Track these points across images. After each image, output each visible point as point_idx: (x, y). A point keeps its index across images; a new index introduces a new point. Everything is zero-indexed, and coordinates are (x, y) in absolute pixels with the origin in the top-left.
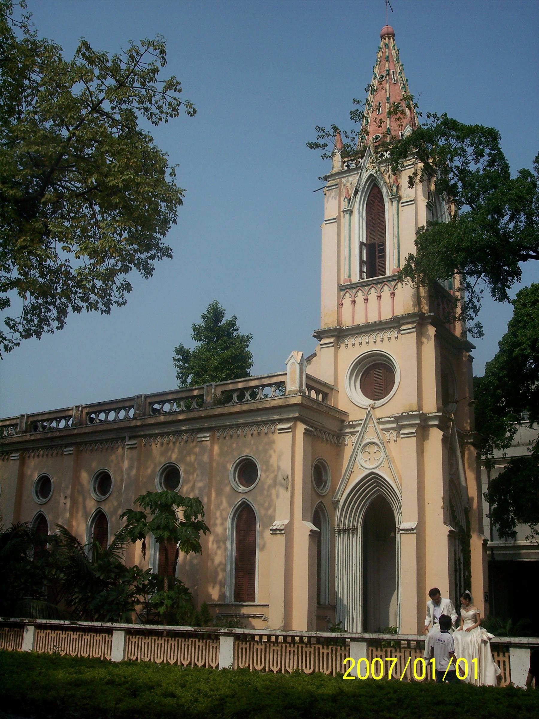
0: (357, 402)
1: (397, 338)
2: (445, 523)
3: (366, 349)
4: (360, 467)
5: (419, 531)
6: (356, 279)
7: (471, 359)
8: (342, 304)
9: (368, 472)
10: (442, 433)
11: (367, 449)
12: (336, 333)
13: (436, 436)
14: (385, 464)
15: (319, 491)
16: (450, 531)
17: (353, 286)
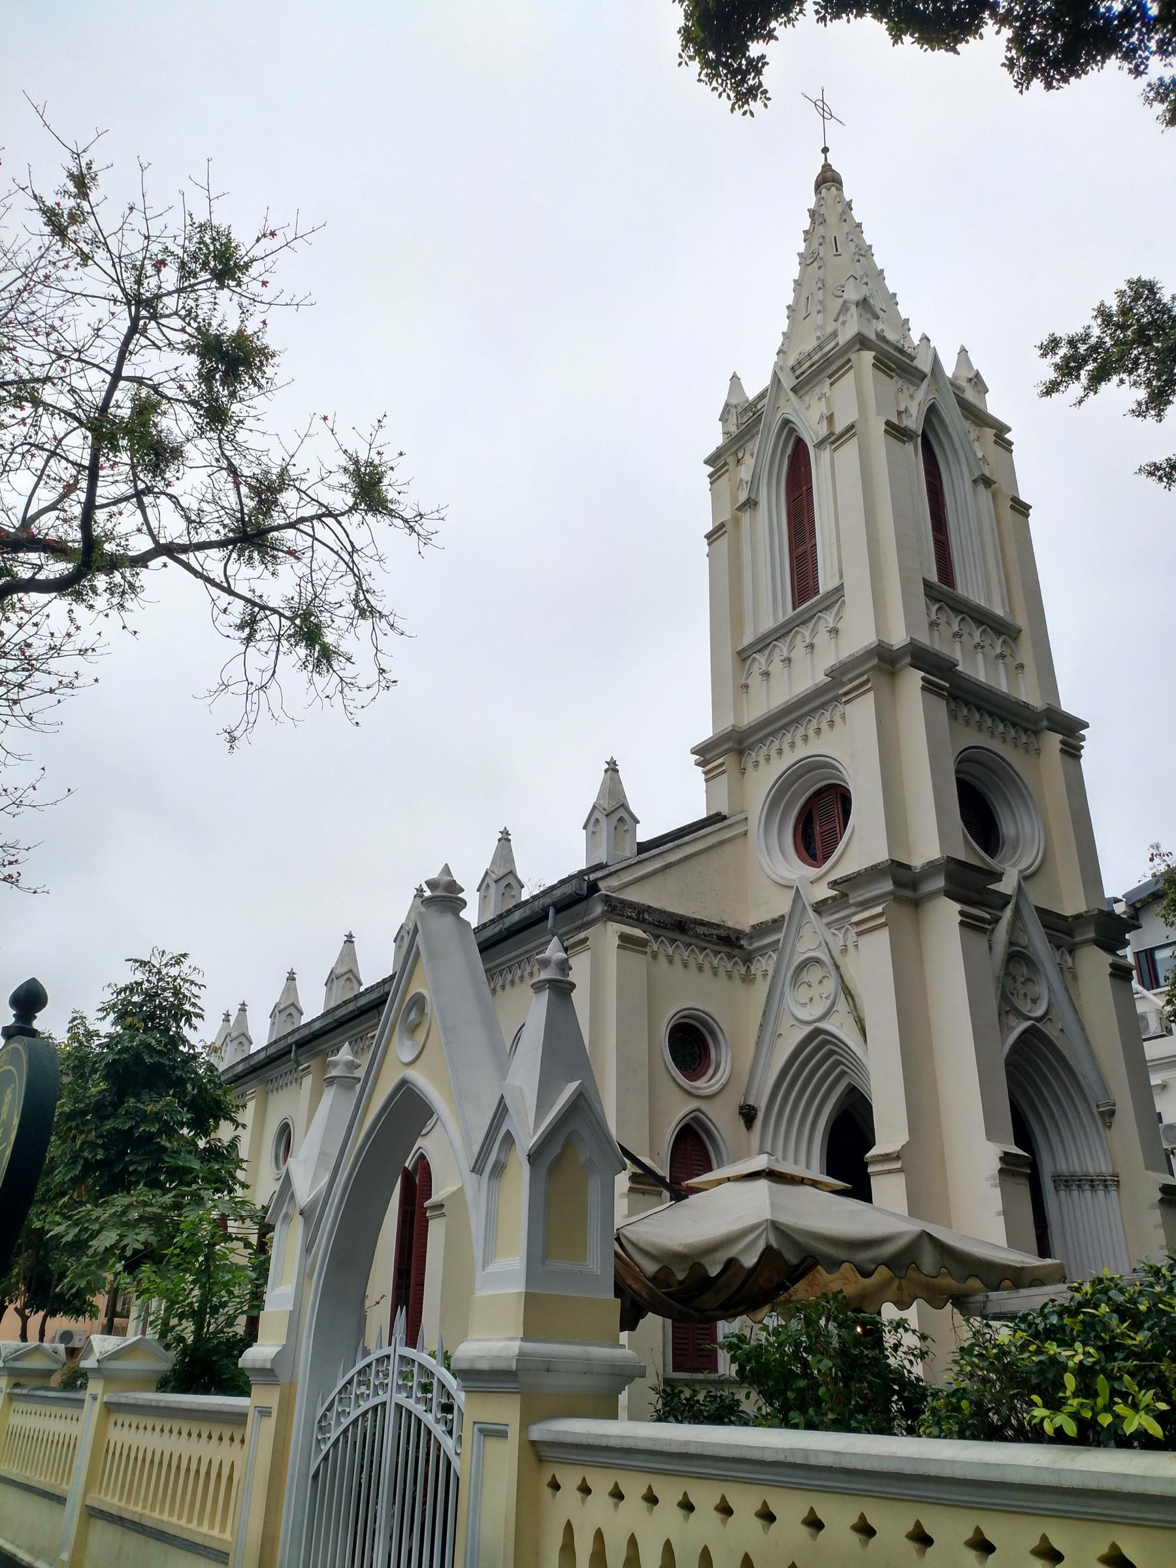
0: (781, 877)
1: (843, 717)
2: (991, 1135)
3: (790, 758)
4: (793, 1022)
6: (768, 624)
7: (1072, 751)
8: (747, 686)
9: (808, 1029)
10: (958, 907)
11: (806, 976)
12: (730, 744)
13: (946, 915)
14: (842, 1005)
15: (697, 1084)
16: (1006, 1158)
17: (764, 643)
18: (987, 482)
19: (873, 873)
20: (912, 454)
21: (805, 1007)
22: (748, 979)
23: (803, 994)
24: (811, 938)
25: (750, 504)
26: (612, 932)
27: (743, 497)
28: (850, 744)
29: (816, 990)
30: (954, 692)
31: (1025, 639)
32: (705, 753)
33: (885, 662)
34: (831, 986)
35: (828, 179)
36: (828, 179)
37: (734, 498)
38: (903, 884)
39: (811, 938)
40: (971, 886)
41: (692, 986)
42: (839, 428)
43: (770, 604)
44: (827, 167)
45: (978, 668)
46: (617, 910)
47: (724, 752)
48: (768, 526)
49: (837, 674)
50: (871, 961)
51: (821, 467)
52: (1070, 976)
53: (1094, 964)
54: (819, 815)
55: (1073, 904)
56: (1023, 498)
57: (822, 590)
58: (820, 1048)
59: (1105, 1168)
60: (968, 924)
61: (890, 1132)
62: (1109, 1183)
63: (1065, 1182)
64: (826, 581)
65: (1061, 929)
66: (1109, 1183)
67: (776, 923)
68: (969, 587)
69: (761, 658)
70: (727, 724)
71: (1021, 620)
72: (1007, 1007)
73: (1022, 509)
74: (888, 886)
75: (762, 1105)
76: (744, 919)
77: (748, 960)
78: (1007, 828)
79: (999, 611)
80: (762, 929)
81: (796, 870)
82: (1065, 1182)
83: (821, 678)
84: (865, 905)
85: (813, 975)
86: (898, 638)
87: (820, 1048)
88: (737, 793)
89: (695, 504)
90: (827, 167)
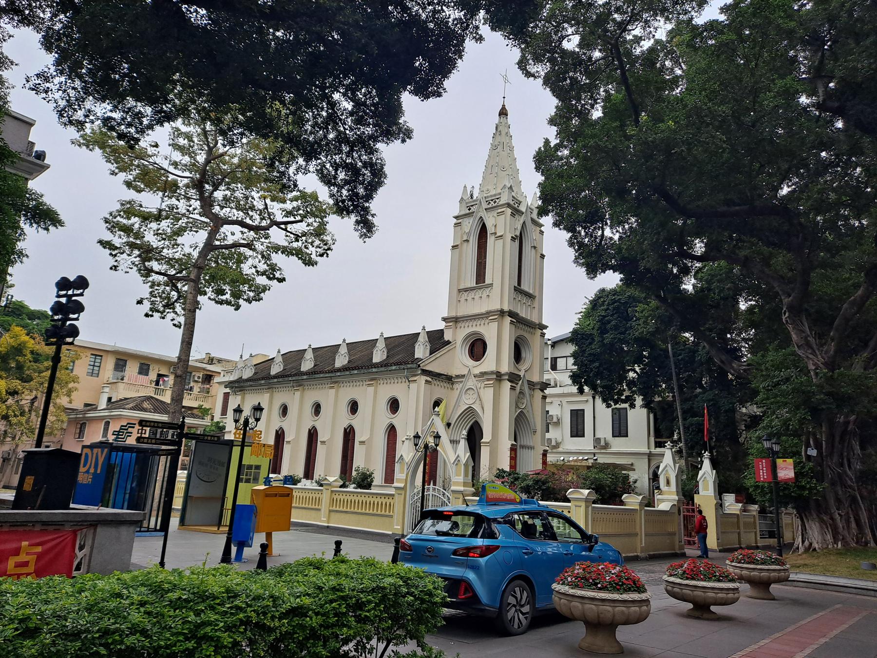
5: (494, 445)
14: (478, 402)
16: (512, 445)
17: (466, 290)
18: (535, 247)
19: (492, 373)
20: (517, 242)
21: (468, 401)
22: (452, 389)
23: (467, 396)
24: (471, 383)
25: (467, 241)
26: (424, 378)
27: (465, 238)
28: (489, 331)
29: (471, 396)
30: (517, 320)
31: (537, 299)
32: (444, 319)
33: (502, 313)
34: (476, 396)
35: (503, 113)
36: (503, 113)
37: (462, 237)
38: (499, 376)
39: (471, 383)
40: (514, 378)
41: (439, 390)
42: (498, 234)
43: (470, 281)
44: (504, 107)
45: (523, 313)
46: (425, 372)
47: (453, 320)
48: (471, 250)
49: (488, 314)
50: (488, 394)
51: (491, 240)
52: (532, 396)
53: (538, 394)
54: (477, 348)
55: (536, 379)
56: (544, 253)
57: (487, 282)
58: (470, 411)
59: (532, 444)
60: (513, 388)
61: (487, 437)
62: (531, 448)
63: (522, 447)
64: (488, 281)
65: (531, 385)
66: (531, 448)
67: (463, 376)
68: (525, 287)
69: (466, 294)
70: (453, 314)
71: (537, 294)
72: (517, 406)
73: (543, 256)
74: (495, 377)
75: (453, 423)
76: (453, 372)
77: (452, 384)
78: (523, 355)
79: (531, 292)
80: (458, 376)
81: (471, 363)
82: (522, 447)
83: (483, 311)
84: (488, 380)
85: (471, 392)
86: (506, 308)
87: (470, 411)
88: (454, 334)
89: (448, 237)
90: (504, 107)
